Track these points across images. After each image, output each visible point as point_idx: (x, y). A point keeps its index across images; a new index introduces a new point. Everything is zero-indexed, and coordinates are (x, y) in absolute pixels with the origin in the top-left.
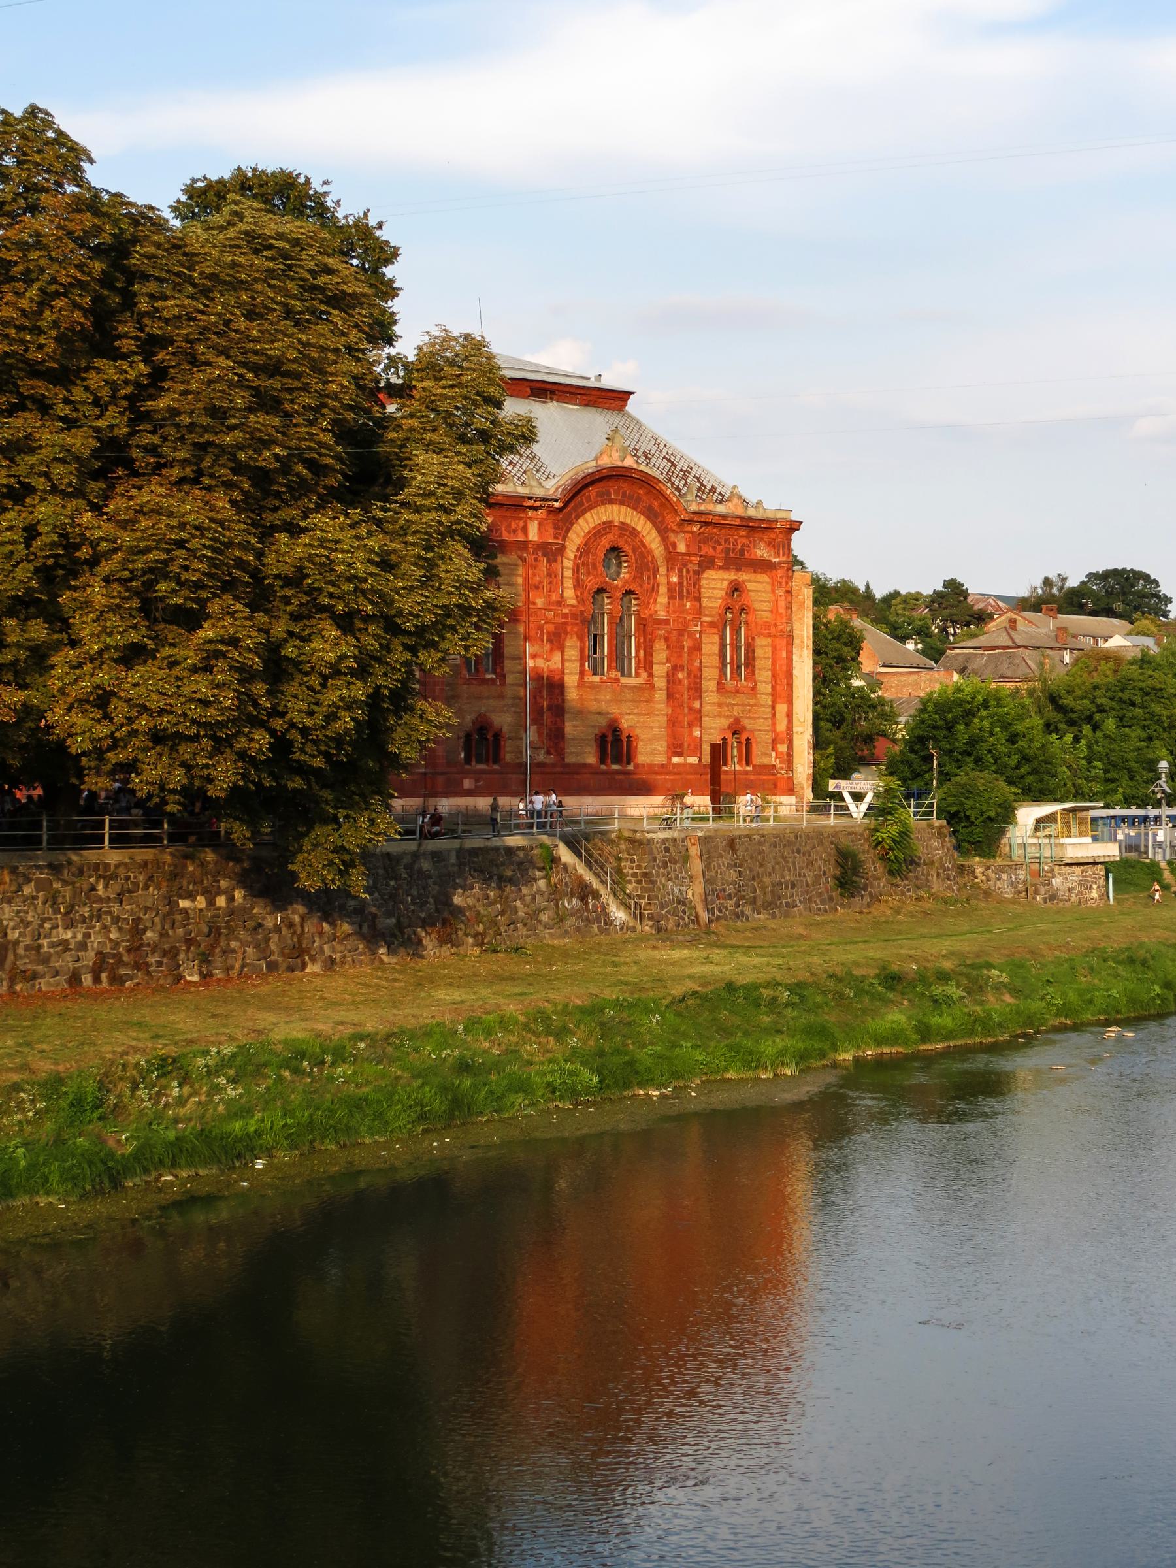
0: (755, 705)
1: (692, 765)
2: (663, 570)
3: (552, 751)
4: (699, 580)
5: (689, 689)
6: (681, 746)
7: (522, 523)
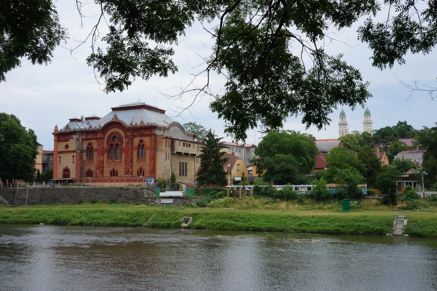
1: (130, 177)
2: (124, 139)
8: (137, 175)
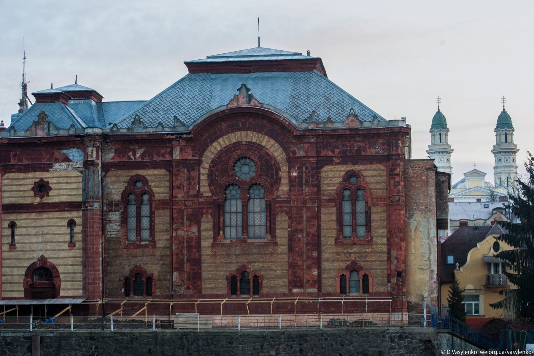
0: (371, 252)
1: (310, 294)
2: (284, 169)
3: (191, 286)
4: (320, 173)
5: (307, 245)
6: (301, 281)
8: (338, 290)
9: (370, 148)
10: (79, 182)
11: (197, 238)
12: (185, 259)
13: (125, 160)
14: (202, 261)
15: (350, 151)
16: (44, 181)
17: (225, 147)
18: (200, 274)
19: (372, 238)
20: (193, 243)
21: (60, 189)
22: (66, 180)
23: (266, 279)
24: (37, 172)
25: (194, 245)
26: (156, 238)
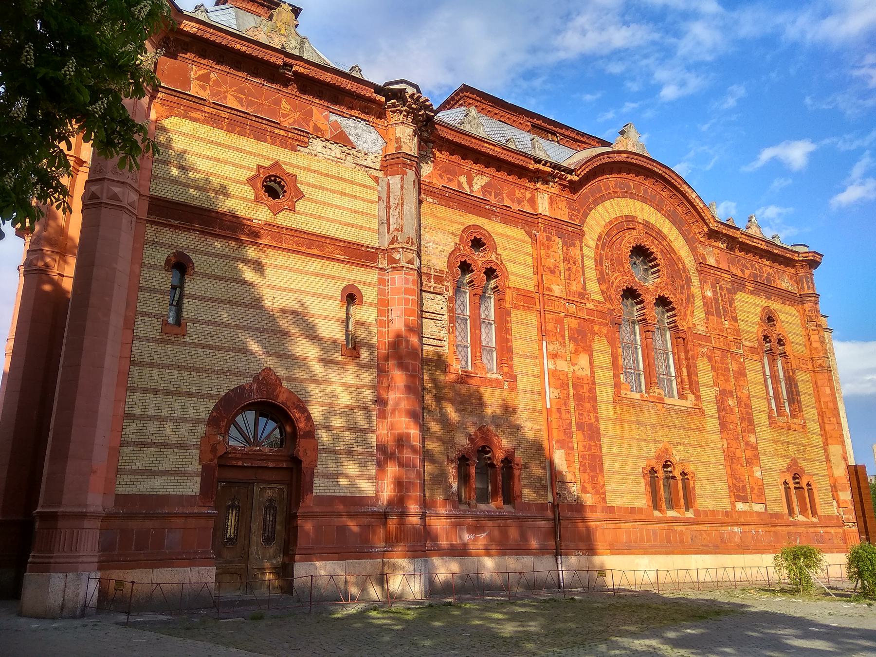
2: (695, 281)
5: (742, 420)
7: (528, 195)
9: (779, 279)
10: (372, 202)
11: (589, 382)
12: (574, 424)
13: (454, 186)
14: (602, 432)
15: (761, 277)
16: (283, 170)
17: (616, 219)
18: (601, 457)
19: (805, 422)
20: (585, 390)
21: (325, 204)
22: (339, 186)
23: (699, 479)
24: (265, 141)
25: (586, 395)
26: (515, 368)
